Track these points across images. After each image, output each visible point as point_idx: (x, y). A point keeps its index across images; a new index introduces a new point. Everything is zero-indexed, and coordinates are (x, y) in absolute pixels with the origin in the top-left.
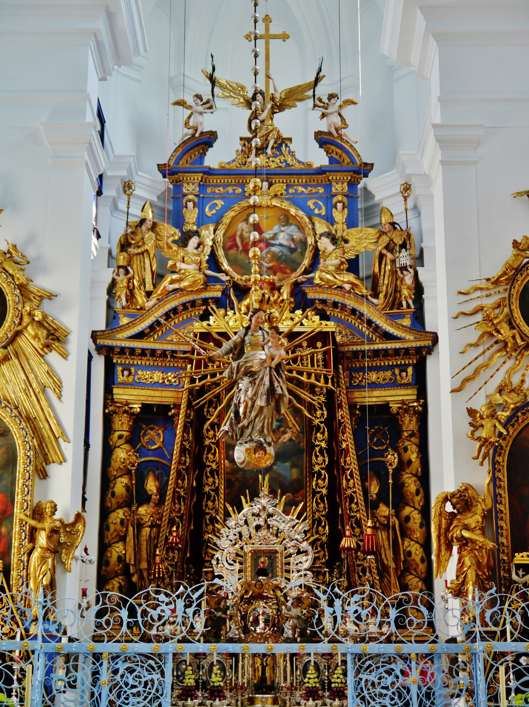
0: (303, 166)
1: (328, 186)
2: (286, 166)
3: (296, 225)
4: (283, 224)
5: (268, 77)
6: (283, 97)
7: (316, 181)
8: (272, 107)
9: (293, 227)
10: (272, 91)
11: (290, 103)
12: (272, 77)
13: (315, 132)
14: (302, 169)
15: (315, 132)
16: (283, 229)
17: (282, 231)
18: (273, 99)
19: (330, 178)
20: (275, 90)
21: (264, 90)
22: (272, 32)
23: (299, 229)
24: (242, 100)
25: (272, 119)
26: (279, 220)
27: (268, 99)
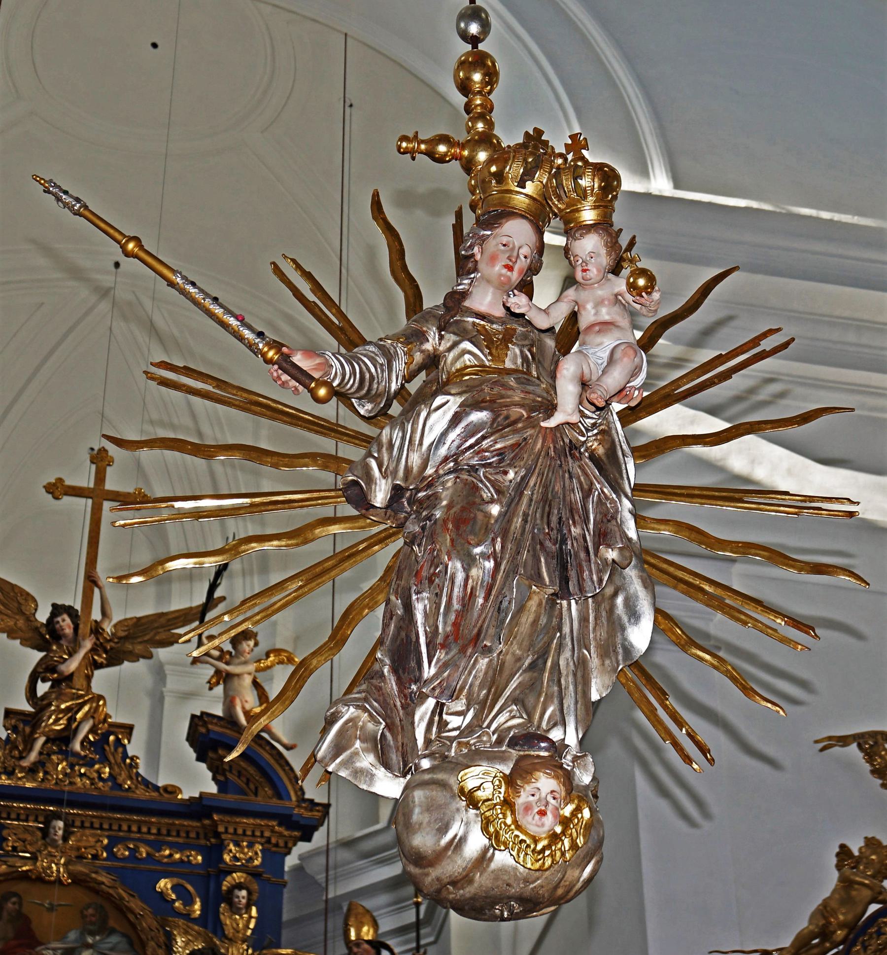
0: (155, 794)
1: (214, 852)
2: (112, 788)
3: (124, 935)
4: (91, 927)
5: (91, 581)
6: (122, 634)
7: (183, 834)
8: (93, 650)
9: (114, 939)
10: (96, 615)
11: (139, 648)
12: (100, 583)
13: (193, 717)
14: (152, 801)
15: (193, 717)
16: (90, 940)
17: (88, 946)
18: (97, 629)
19: (221, 829)
20: (104, 613)
21: (78, 606)
22: (110, 485)
23: (131, 944)
24: (21, 623)
25: (89, 678)
26: (84, 917)
27: (84, 629)
